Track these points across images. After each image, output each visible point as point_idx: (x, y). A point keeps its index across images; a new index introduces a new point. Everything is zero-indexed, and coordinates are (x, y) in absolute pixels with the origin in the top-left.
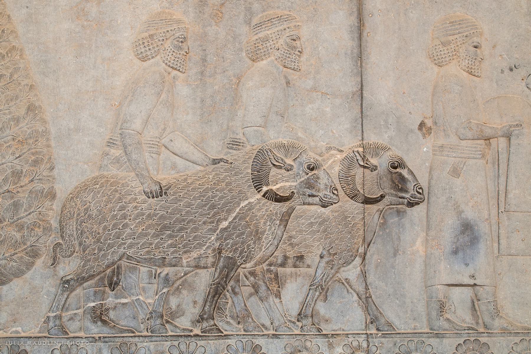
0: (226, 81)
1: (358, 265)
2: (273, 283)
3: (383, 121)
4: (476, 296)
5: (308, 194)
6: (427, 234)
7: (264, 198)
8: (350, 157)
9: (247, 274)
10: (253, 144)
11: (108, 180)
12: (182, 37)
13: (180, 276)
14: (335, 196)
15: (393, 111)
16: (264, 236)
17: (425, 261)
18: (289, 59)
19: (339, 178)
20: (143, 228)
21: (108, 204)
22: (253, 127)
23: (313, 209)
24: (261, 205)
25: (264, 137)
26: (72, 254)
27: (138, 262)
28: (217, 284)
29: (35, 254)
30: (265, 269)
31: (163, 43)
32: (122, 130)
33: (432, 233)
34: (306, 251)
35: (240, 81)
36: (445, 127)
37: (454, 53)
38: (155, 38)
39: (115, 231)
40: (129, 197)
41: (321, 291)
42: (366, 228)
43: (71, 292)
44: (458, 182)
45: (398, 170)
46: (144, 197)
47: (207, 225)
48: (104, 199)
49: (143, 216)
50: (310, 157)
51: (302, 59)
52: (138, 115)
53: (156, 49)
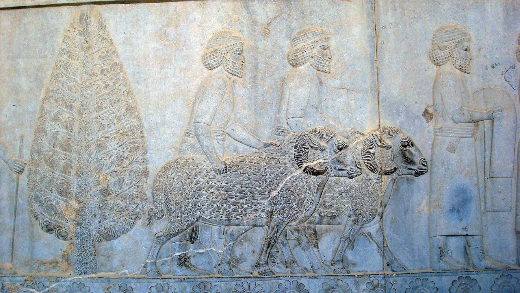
0: (273, 83)
4: (468, 243)
6: (430, 197)
8: (370, 139)
9: (293, 230)
10: (295, 131)
12: (239, 50)
15: (403, 102)
17: (428, 218)
18: (321, 64)
19: (362, 156)
20: (213, 197)
25: (303, 125)
26: (162, 217)
29: (136, 218)
33: (435, 196)
37: (449, 56)
39: (193, 200)
40: (203, 174)
42: (383, 193)
43: (162, 245)
44: (454, 156)
45: (407, 148)
46: (214, 173)
51: (331, 64)
53: (220, 60)
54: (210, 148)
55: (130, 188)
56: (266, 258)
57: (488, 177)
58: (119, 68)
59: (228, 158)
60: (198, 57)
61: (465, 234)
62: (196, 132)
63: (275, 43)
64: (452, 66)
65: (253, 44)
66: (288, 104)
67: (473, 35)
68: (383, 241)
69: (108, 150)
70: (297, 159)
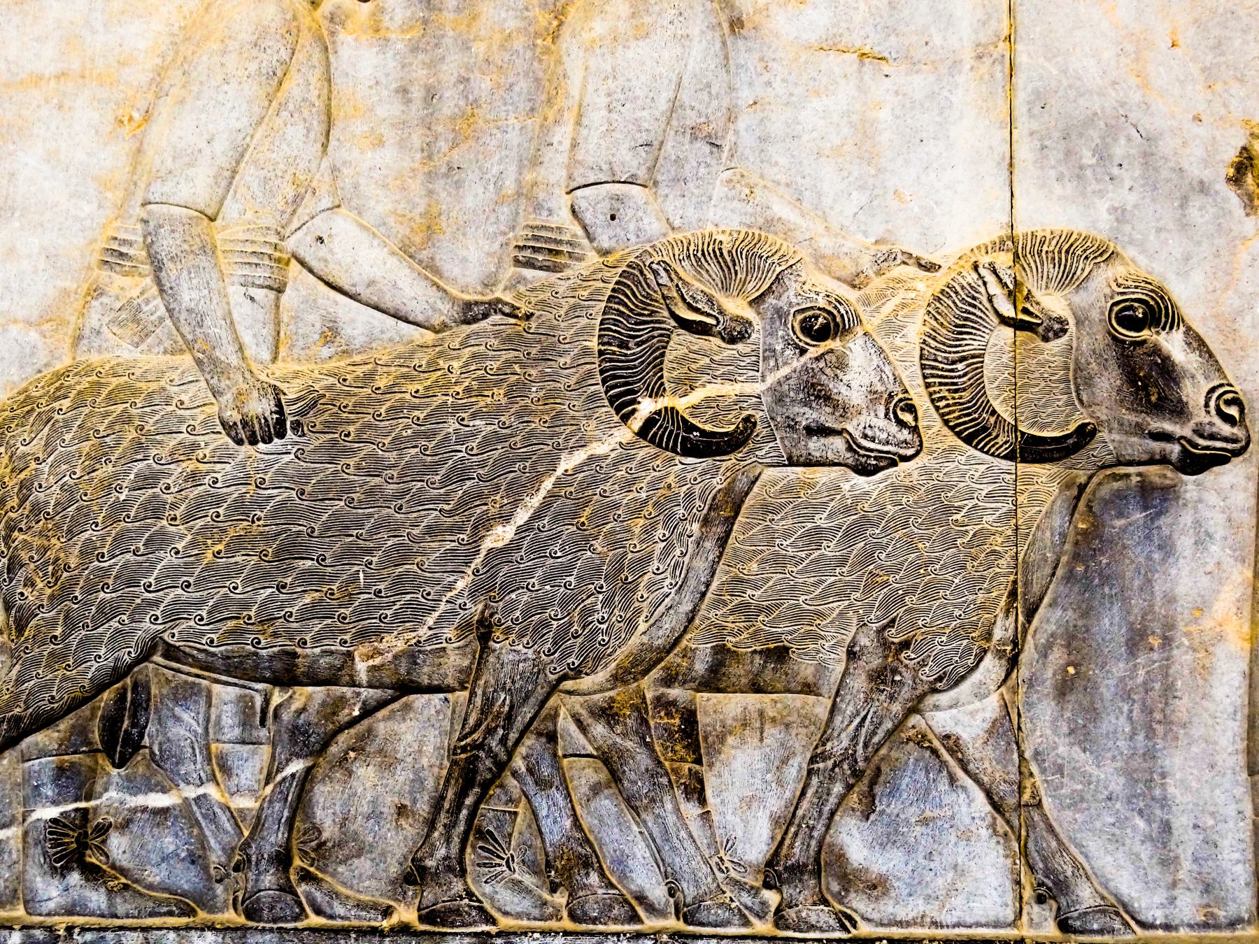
1: (993, 688)
2: (678, 748)
3: (1090, 154)
5: (804, 423)
8: (963, 288)
11: (102, 381)
13: (347, 719)
14: (905, 432)
15: (1131, 115)
16: (646, 578)
19: (923, 367)
20: (220, 547)
21: (98, 466)
23: (824, 480)
25: (646, 221)
27: (201, 669)
30: (649, 696)
32: (149, 207)
34: (795, 631)
39: (121, 560)
40: (173, 441)
41: (851, 781)
47: (439, 538)
48: (86, 447)
50: (814, 289)
52: (200, 151)
54: (208, 322)
62: (149, 247)
66: (578, 123)
68: (1014, 777)
70: (615, 377)
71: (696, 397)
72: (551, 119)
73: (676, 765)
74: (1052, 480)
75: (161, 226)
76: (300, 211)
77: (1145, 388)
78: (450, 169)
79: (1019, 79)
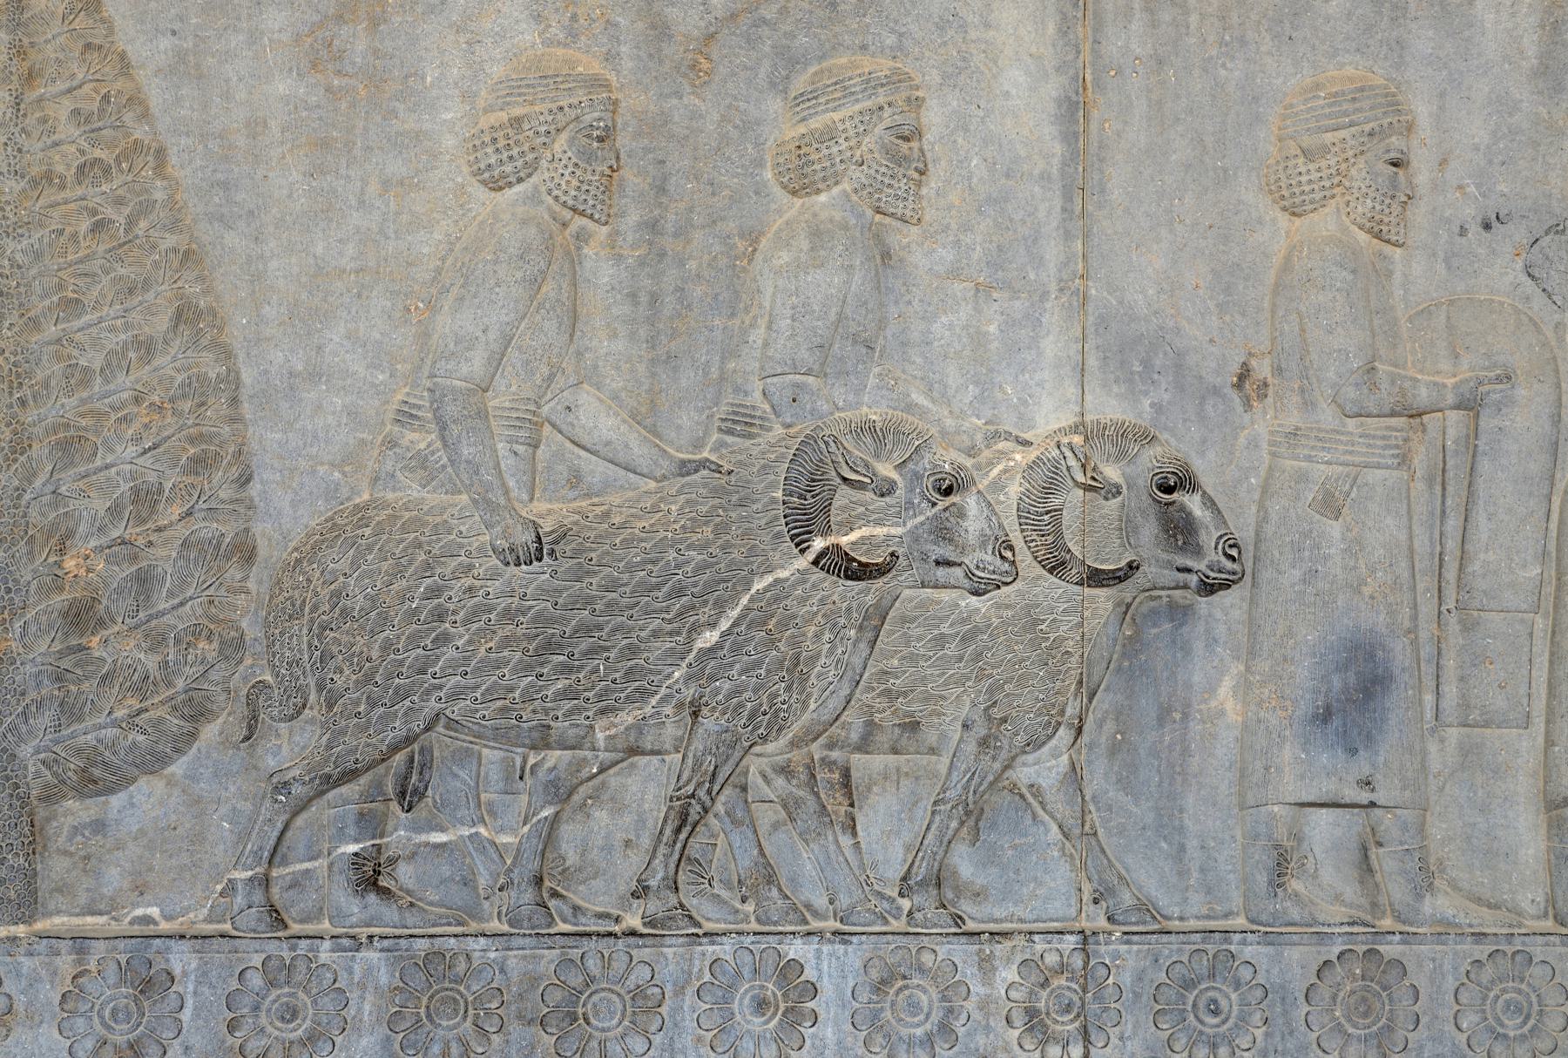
0: (717, 248)
2: (837, 795)
6: (1248, 669)
7: (815, 569)
9: (769, 771)
14: (1007, 565)
15: (1167, 336)
16: (816, 670)
19: (1019, 517)
22: (791, 376)
24: (808, 585)
25: (819, 403)
26: (299, 713)
28: (688, 797)
29: (197, 712)
30: (816, 757)
31: (547, 140)
33: (1263, 666)
35: (755, 250)
36: (1305, 382)
37: (1336, 181)
38: (526, 126)
39: (413, 654)
40: (453, 563)
41: (964, 818)
43: (295, 814)
44: (1335, 529)
45: (1175, 496)
48: (385, 566)
49: (490, 612)
51: (924, 191)
53: (530, 157)
55: (182, 604)
56: (672, 866)
57: (1452, 606)
58: (151, 164)
59: (550, 512)
60: (449, 142)
61: (1365, 802)
63: (729, 106)
64: (1344, 218)
65: (652, 107)
66: (769, 328)
67: (1422, 110)
68: (1079, 815)
69: (98, 463)
71: (854, 536)
72: (747, 322)
73: (835, 808)
74: (1108, 600)
75: (445, 396)
76: (553, 386)
77: (1174, 536)
78: (669, 357)
79: (1090, 308)
